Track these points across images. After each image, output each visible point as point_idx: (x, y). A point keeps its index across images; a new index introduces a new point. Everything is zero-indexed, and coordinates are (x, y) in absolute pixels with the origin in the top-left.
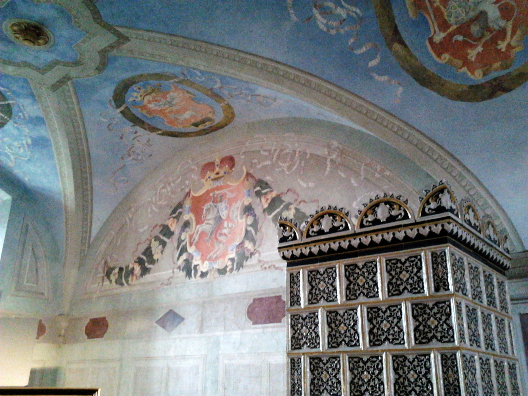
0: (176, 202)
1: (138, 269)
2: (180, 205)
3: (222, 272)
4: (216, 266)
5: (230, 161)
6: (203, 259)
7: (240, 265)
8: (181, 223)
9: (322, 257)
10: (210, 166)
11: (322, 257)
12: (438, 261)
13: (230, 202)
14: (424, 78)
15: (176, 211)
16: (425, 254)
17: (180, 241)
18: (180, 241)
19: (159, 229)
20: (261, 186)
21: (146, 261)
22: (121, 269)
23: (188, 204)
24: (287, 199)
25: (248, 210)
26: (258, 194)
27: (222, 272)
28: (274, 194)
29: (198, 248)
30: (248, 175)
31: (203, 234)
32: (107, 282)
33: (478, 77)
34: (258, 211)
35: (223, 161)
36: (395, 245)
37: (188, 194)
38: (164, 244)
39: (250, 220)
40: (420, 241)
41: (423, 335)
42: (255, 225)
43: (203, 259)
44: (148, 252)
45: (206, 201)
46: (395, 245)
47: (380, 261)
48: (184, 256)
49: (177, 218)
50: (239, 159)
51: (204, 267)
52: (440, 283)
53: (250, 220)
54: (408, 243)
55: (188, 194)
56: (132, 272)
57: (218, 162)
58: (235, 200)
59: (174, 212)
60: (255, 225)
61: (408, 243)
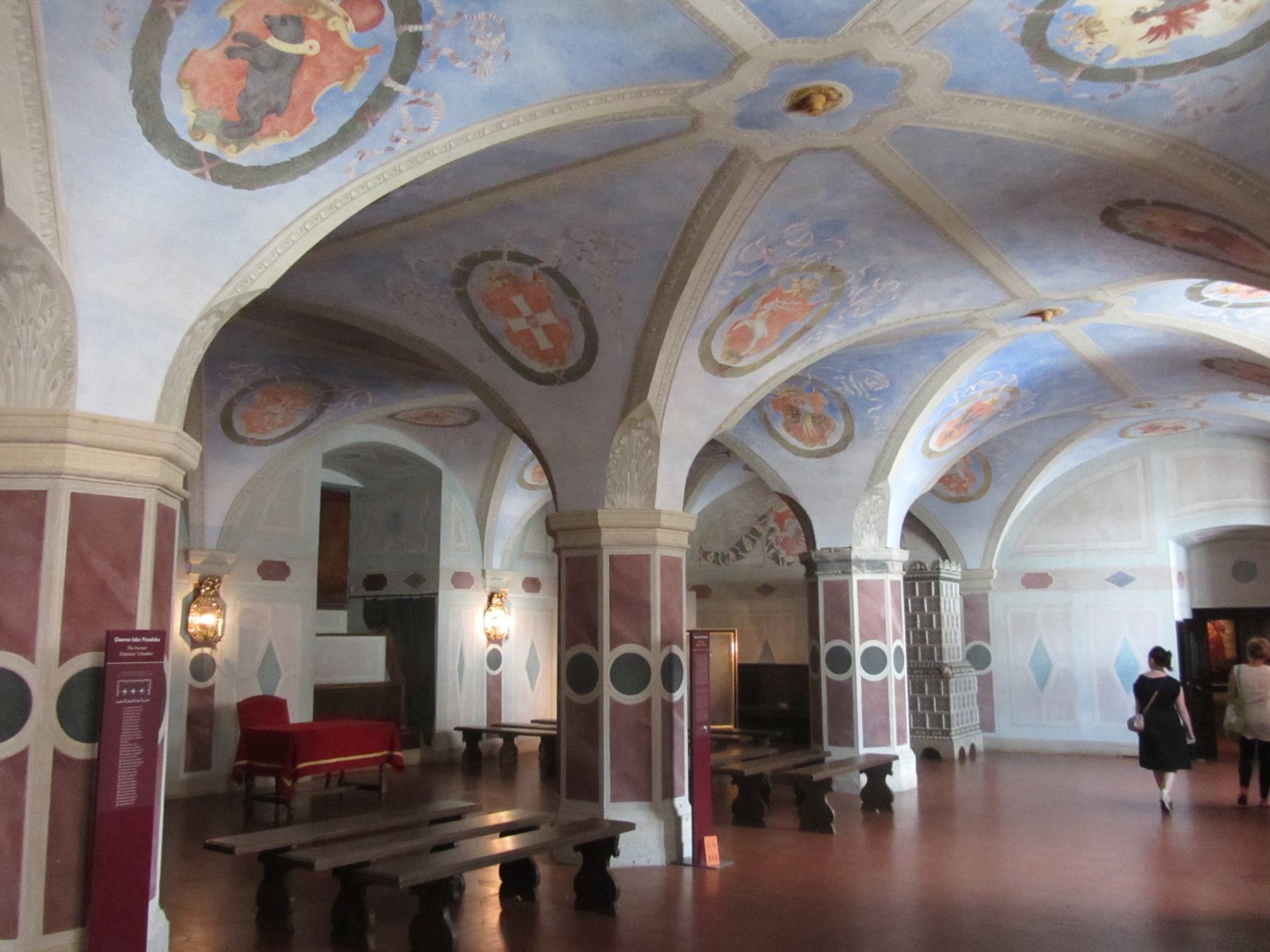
0: (761, 514)
1: (732, 555)
2: (764, 517)
6: (788, 554)
15: (762, 519)
18: (768, 541)
22: (716, 554)
31: (786, 539)
32: (704, 562)
33: (953, 494)
36: (922, 579)
38: (754, 541)
43: (788, 554)
44: (740, 544)
48: (773, 551)
49: (765, 524)
54: (926, 578)
59: (760, 519)
61: (926, 578)
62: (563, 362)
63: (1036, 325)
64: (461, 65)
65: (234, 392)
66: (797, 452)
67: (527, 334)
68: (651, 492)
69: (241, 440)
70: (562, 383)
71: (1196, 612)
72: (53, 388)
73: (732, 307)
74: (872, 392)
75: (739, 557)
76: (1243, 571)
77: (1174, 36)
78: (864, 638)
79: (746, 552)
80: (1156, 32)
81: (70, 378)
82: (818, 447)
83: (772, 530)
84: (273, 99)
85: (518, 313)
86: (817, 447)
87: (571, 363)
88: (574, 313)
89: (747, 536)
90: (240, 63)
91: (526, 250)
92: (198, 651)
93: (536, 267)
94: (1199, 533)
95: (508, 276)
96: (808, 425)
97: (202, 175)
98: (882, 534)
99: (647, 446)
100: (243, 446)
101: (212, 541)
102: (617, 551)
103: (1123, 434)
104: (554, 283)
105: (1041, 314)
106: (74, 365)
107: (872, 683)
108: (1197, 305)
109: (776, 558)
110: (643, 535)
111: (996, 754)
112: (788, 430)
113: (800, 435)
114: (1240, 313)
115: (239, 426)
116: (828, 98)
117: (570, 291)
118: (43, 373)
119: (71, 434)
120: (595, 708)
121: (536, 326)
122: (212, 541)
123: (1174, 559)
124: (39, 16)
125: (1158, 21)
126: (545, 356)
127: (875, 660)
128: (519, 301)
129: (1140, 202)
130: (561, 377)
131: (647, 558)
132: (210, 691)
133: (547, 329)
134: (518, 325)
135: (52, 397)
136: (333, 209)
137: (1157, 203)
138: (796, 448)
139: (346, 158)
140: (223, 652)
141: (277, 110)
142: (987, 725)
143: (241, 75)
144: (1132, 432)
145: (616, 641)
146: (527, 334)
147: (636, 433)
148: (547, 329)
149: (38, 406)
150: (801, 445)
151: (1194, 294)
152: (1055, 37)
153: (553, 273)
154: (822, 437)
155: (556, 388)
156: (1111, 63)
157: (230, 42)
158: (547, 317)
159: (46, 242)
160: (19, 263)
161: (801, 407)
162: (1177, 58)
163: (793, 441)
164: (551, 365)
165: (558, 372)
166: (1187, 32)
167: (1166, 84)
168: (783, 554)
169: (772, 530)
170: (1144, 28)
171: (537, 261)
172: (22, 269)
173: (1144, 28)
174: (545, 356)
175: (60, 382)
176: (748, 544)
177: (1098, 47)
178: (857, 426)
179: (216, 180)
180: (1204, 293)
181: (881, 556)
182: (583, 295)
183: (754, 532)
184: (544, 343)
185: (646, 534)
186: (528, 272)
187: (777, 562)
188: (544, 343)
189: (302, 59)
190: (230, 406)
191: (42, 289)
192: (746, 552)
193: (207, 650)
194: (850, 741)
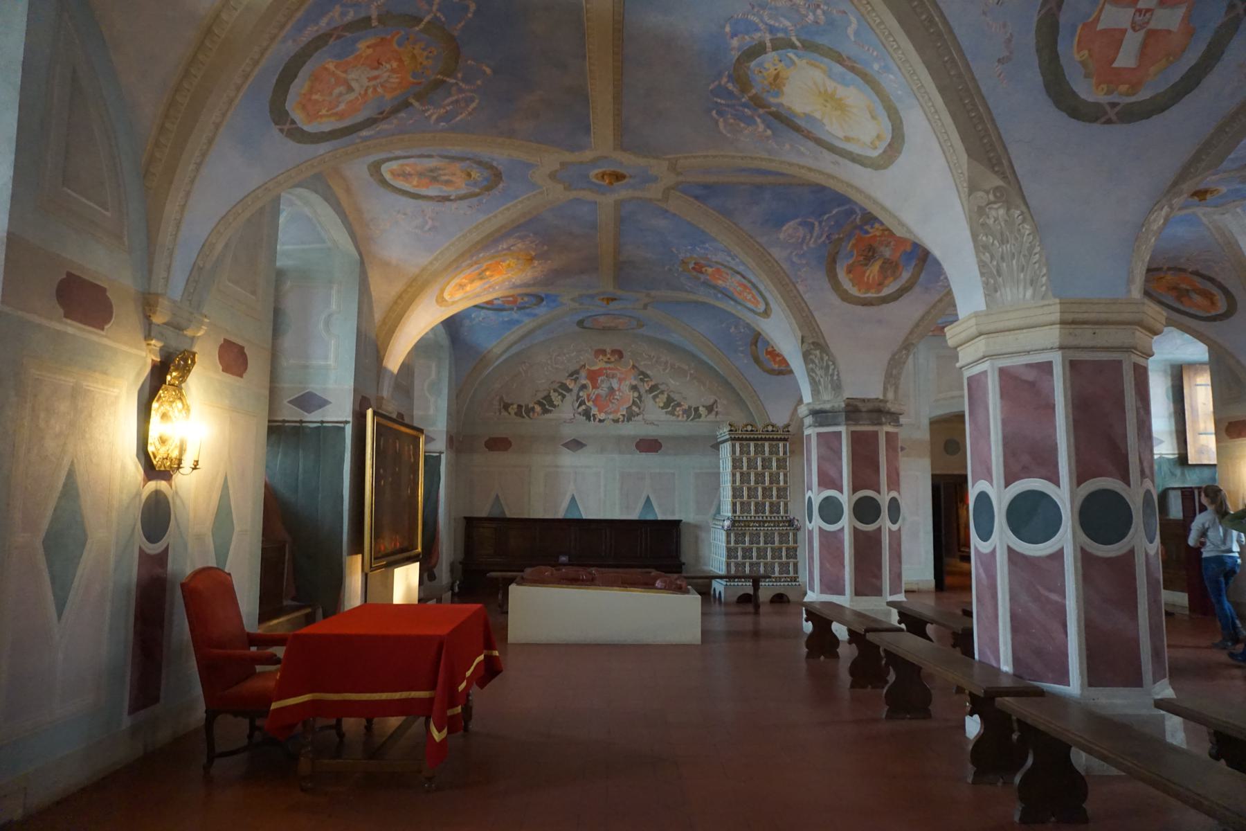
0: (572, 369)
1: (538, 408)
2: (577, 372)
3: (617, 421)
4: (611, 417)
5: (619, 354)
6: (600, 411)
7: (629, 420)
8: (578, 385)
9: (746, 439)
10: (603, 352)
11: (746, 439)
12: (785, 446)
13: (620, 380)
14: (757, 360)
15: (574, 374)
16: (781, 445)
17: (578, 397)
19: (556, 386)
20: (644, 376)
21: (547, 404)
22: (520, 406)
23: (583, 373)
24: (662, 387)
25: (634, 388)
26: (641, 380)
27: (617, 421)
28: (651, 383)
29: (596, 405)
30: (634, 367)
32: (504, 413)
33: (776, 367)
34: (642, 391)
35: (614, 352)
37: (584, 366)
38: (564, 396)
39: (636, 394)
40: (781, 440)
41: (778, 467)
42: (640, 397)
43: (600, 411)
44: (548, 398)
45: (601, 375)
46: (773, 439)
47: (767, 444)
48: (584, 407)
49: (576, 380)
50: (627, 354)
51: (602, 416)
52: (785, 453)
53: (636, 394)
54: (777, 439)
55: (584, 366)
56: (533, 409)
57: (608, 350)
58: (624, 379)
59: (571, 375)
60: (640, 397)
61: (777, 439)
66: (846, 297)
70: (1109, 122)
75: (546, 411)
79: (554, 406)
83: (584, 387)
86: (869, 295)
87: (1144, 95)
89: (555, 391)
92: (152, 485)
96: (874, 270)
100: (275, 130)
109: (587, 414)
112: (849, 271)
113: (857, 282)
132: (161, 559)
138: (846, 291)
140: (191, 488)
150: (854, 291)
154: (880, 285)
155: (1096, 127)
161: (882, 249)
163: (847, 285)
165: (1113, 105)
168: (594, 411)
169: (584, 387)
174: (1110, 76)
176: (555, 398)
178: (922, 275)
183: (564, 387)
187: (588, 418)
192: (554, 406)
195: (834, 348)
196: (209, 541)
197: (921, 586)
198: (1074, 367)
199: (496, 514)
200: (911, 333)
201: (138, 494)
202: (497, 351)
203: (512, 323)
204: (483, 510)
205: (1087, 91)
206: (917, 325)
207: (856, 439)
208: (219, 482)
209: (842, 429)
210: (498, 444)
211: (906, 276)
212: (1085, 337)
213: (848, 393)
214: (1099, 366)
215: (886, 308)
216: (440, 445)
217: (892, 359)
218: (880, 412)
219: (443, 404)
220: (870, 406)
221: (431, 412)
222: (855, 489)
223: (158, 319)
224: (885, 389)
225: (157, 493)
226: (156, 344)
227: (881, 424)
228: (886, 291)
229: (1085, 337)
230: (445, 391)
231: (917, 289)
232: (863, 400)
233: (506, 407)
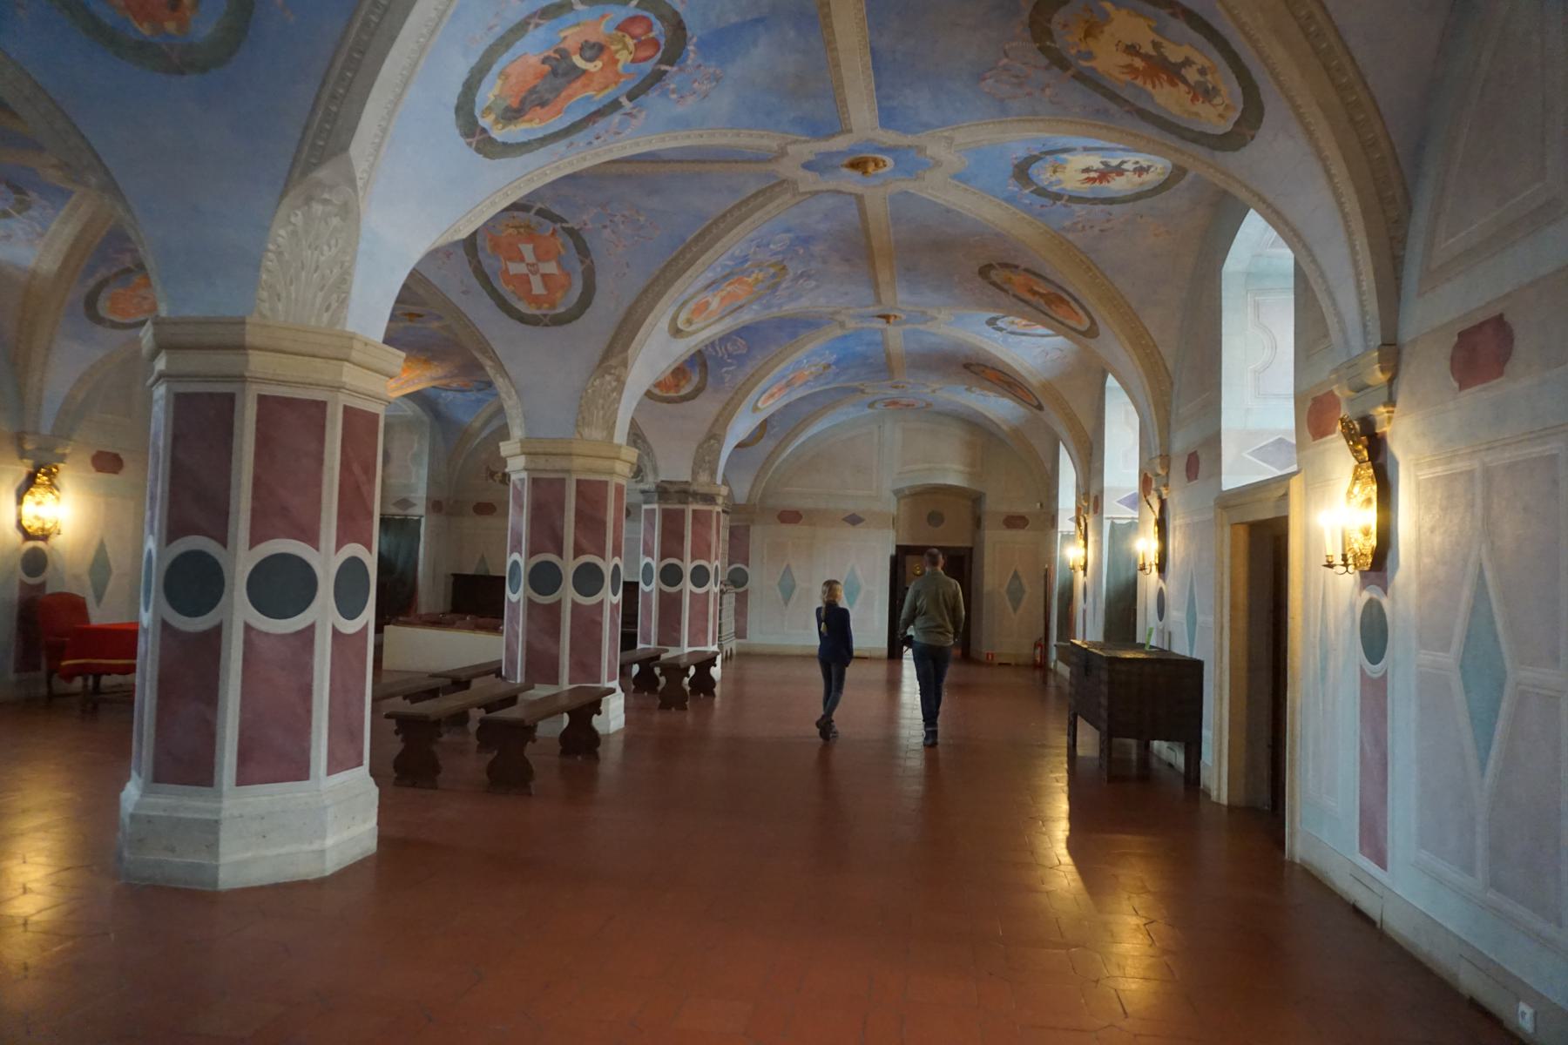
62: (553, 306)
63: (880, 324)
64: (674, 96)
65: (115, 270)
67: (524, 280)
68: (610, 428)
69: (99, 320)
71: (898, 547)
72: (327, 309)
73: (707, 287)
74: (730, 356)
76: (935, 519)
77: (1097, 184)
78: (694, 558)
80: (1089, 179)
81: (343, 302)
82: (672, 394)
84: (547, 96)
85: (522, 260)
87: (561, 310)
88: (579, 268)
90: (547, 68)
91: (557, 210)
92: (31, 544)
93: (558, 226)
94: (909, 488)
95: (528, 226)
97: (470, 144)
98: (713, 473)
99: (613, 390)
100: (99, 328)
101: (46, 426)
102: (583, 477)
103: (871, 405)
104: (570, 242)
105: (886, 317)
106: (348, 293)
107: (669, 594)
108: (989, 329)
110: (606, 464)
111: (745, 656)
114: (1012, 338)
115: (103, 307)
116: (876, 165)
117: (583, 250)
118: (320, 295)
119: (355, 355)
120: (555, 609)
121: (535, 273)
122: (46, 426)
123: (891, 506)
124: (450, 12)
125: (1093, 175)
126: (536, 300)
127: (700, 576)
128: (527, 250)
129: (1017, 267)
130: (546, 320)
131: (606, 483)
133: (545, 278)
134: (516, 268)
135: (326, 317)
136: (531, 180)
137: (1027, 270)
139: (560, 146)
141: (543, 104)
142: (740, 633)
143: (543, 76)
144: (879, 406)
145: (578, 551)
146: (524, 280)
147: (608, 378)
148: (545, 278)
149: (313, 322)
151: (991, 322)
152: (1033, 171)
153: (573, 233)
154: (677, 387)
156: (1055, 189)
157: (551, 53)
158: (550, 268)
159: (360, 183)
160: (326, 196)
162: (1090, 196)
164: (539, 308)
166: (1105, 184)
167: (1076, 207)
170: (1085, 175)
171: (563, 220)
172: (326, 202)
173: (1085, 175)
175: (334, 305)
177: (1053, 179)
178: (710, 379)
179: (478, 150)
180: (1000, 323)
181: (714, 490)
182: (593, 256)
184: (538, 288)
185: (606, 464)
186: (549, 226)
188: (538, 288)
189: (584, 72)
190: (102, 285)
191: (335, 221)
193: (40, 544)
194: (677, 643)
195: (650, 440)
196: (87, 579)
197: (877, 654)
198: (535, 482)
199: (482, 573)
200: (713, 425)
201: (18, 549)
202: (477, 424)
203: (479, 402)
204: (470, 570)
205: (523, 307)
206: (717, 420)
207: (666, 515)
208: (95, 543)
209: (655, 506)
210: (485, 509)
211: (695, 378)
212: (541, 463)
213: (662, 477)
214: (551, 482)
215: (686, 404)
216: (419, 510)
217: (700, 446)
218: (684, 493)
219: (424, 472)
220: (676, 488)
221: (413, 480)
222: (663, 557)
223: (29, 446)
224: (695, 474)
225: (35, 550)
226: (29, 462)
227: (686, 503)
228: (683, 392)
229: (541, 463)
230: (426, 459)
231: (709, 388)
232: (671, 483)
233: (492, 475)
